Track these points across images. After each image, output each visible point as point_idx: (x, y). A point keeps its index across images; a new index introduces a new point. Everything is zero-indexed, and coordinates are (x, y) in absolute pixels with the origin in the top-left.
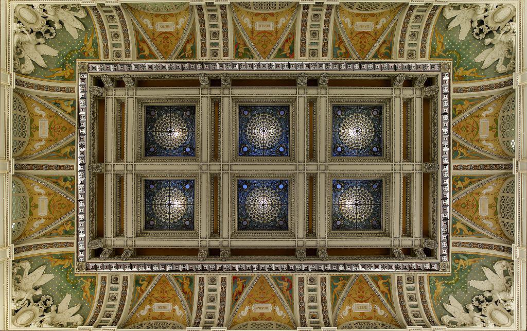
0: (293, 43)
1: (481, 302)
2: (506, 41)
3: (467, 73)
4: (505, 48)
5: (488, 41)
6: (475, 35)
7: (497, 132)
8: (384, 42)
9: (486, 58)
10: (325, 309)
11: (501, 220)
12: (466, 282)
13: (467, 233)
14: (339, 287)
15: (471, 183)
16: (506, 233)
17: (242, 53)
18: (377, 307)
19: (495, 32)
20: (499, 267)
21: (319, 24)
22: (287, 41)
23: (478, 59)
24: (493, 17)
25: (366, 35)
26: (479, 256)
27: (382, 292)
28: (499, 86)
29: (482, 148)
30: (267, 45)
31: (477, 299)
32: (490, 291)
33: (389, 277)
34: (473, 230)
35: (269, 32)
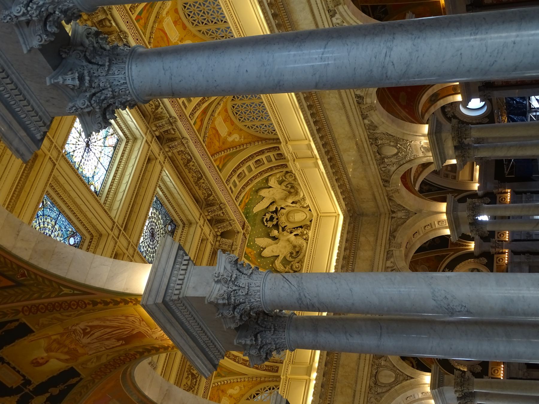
2: (295, 243)
4: (289, 249)
5: (275, 233)
6: (265, 220)
24: (288, 214)
25: (217, 136)
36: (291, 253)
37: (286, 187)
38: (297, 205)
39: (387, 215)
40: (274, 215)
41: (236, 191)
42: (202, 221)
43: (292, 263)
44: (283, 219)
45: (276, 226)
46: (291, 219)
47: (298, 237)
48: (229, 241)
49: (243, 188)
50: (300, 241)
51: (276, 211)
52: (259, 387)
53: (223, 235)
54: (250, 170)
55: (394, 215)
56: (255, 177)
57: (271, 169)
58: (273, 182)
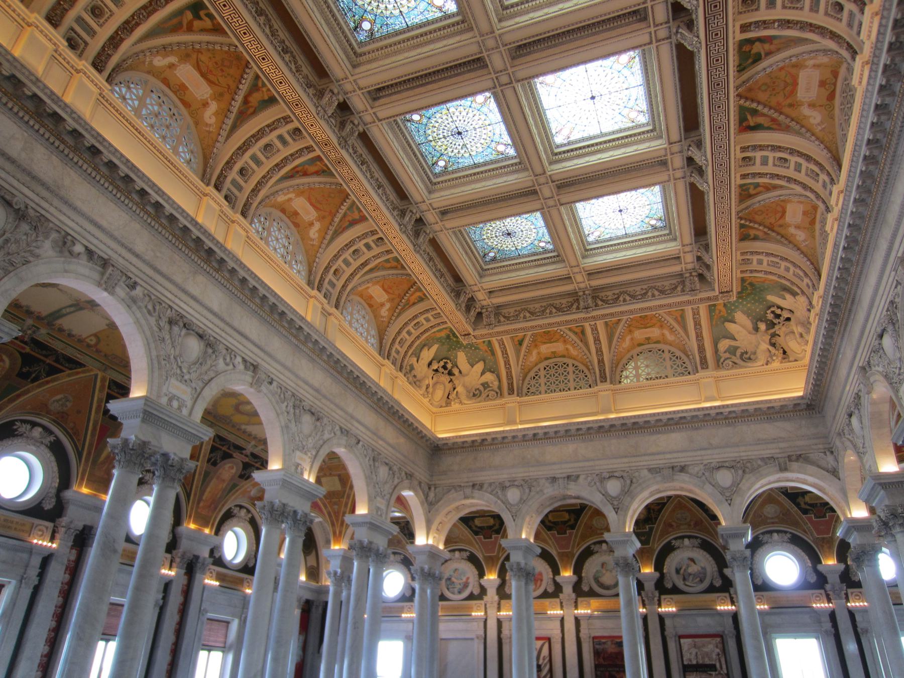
0: (769, 128)
1: (444, 367)
2: (758, 351)
5: (762, 326)
6: (772, 309)
10: (352, 275)
11: (542, 366)
12: (460, 348)
13: (516, 339)
14: (388, 265)
16: (528, 378)
17: (750, 51)
18: (388, 306)
19: (772, 331)
20: (489, 377)
22: (774, 120)
23: (739, 316)
26: (493, 353)
27: (408, 300)
28: (701, 349)
29: (622, 338)
30: (766, 90)
31: (446, 363)
32: (460, 372)
35: (793, 92)
36: (746, 353)
38: (799, 340)
39: (827, 446)
43: (733, 357)
44: (781, 330)
45: (771, 325)
46: (788, 337)
47: (768, 354)
48: (698, 286)
49: (766, 273)
50: (762, 358)
51: (788, 319)
52: (586, 371)
53: (701, 277)
55: (828, 453)
57: (803, 293)
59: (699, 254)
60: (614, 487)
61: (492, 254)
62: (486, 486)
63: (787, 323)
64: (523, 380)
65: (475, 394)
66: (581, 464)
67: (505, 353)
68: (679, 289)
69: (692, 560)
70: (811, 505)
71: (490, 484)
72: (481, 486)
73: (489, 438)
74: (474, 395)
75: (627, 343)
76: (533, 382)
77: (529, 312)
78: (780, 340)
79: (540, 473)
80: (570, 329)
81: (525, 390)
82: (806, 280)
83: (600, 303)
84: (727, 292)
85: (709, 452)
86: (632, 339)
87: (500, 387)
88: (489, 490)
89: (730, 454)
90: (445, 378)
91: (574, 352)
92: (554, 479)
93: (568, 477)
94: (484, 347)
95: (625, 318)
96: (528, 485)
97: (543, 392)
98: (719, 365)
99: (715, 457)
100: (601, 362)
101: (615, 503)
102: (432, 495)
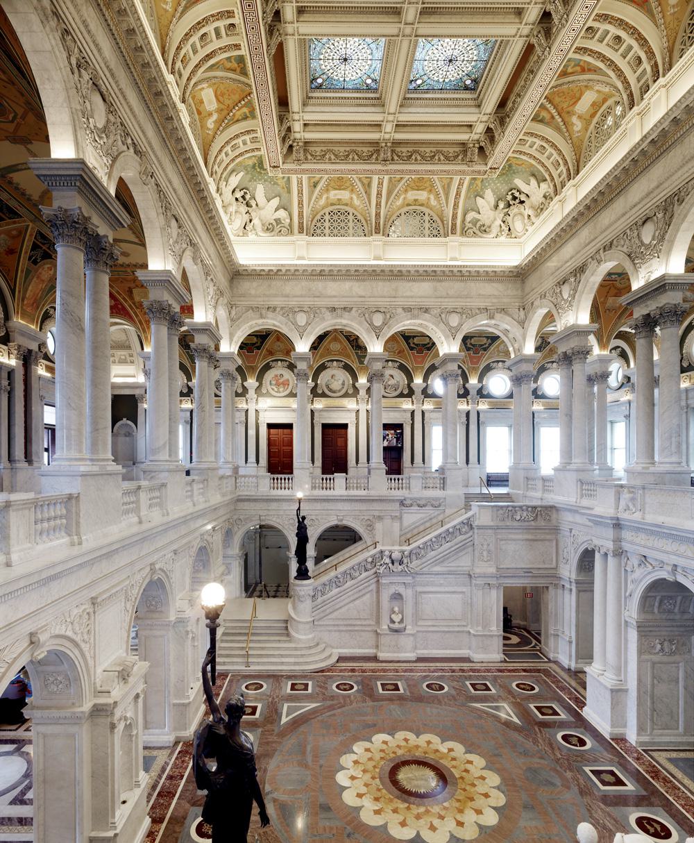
2: (493, 226)
3: (479, 182)
4: (487, 223)
5: (502, 205)
7: (410, 205)
8: (553, 117)
9: (486, 203)
13: (312, 181)
15: (363, 184)
16: (315, 220)
20: (282, 214)
21: (625, 57)
24: (521, 214)
25: (574, 100)
26: (289, 191)
28: (454, 217)
32: (257, 205)
33: (254, 117)
34: (315, 186)
36: (484, 225)
37: (542, 203)
38: (526, 221)
39: (521, 304)
40: (518, 201)
41: (526, 149)
42: (485, 118)
44: (514, 210)
51: (522, 202)
52: (363, 221)
53: (481, 149)
54: (549, 158)
55: (521, 309)
56: (543, 165)
57: (553, 179)
58: (544, 187)
59: (492, 126)
60: (378, 320)
61: (320, 81)
62: (278, 309)
63: (520, 205)
64: (312, 221)
65: (269, 229)
66: (355, 299)
67: (300, 192)
68: (460, 158)
69: (392, 376)
70: (473, 345)
71: (282, 308)
72: (275, 309)
73: (284, 269)
74: (268, 229)
75: (399, 202)
76: (319, 224)
77: (336, 155)
78: (509, 219)
79: (323, 303)
80: (360, 179)
81: (312, 232)
82: (562, 168)
83: (396, 158)
84: (495, 168)
85: (446, 300)
86: (405, 198)
87: (290, 225)
88: (281, 313)
89: (459, 304)
90: (243, 209)
91: (356, 202)
92: (334, 309)
93: (345, 308)
94: (282, 183)
95: (408, 177)
96: (313, 312)
97: (327, 235)
98: (464, 233)
99: (450, 304)
100: (378, 215)
101: (377, 331)
102: (233, 313)
